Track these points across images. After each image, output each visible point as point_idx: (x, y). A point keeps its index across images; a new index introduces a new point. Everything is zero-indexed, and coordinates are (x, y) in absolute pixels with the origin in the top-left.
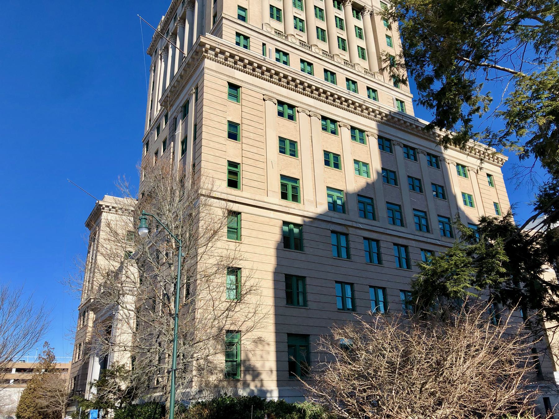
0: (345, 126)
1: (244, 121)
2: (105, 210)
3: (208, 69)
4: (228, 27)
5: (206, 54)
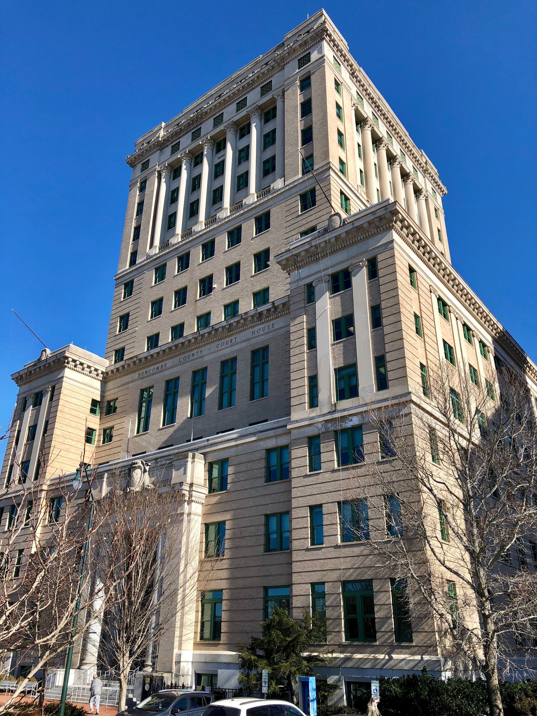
1: (424, 315)
2: (69, 365)
3: (396, 243)
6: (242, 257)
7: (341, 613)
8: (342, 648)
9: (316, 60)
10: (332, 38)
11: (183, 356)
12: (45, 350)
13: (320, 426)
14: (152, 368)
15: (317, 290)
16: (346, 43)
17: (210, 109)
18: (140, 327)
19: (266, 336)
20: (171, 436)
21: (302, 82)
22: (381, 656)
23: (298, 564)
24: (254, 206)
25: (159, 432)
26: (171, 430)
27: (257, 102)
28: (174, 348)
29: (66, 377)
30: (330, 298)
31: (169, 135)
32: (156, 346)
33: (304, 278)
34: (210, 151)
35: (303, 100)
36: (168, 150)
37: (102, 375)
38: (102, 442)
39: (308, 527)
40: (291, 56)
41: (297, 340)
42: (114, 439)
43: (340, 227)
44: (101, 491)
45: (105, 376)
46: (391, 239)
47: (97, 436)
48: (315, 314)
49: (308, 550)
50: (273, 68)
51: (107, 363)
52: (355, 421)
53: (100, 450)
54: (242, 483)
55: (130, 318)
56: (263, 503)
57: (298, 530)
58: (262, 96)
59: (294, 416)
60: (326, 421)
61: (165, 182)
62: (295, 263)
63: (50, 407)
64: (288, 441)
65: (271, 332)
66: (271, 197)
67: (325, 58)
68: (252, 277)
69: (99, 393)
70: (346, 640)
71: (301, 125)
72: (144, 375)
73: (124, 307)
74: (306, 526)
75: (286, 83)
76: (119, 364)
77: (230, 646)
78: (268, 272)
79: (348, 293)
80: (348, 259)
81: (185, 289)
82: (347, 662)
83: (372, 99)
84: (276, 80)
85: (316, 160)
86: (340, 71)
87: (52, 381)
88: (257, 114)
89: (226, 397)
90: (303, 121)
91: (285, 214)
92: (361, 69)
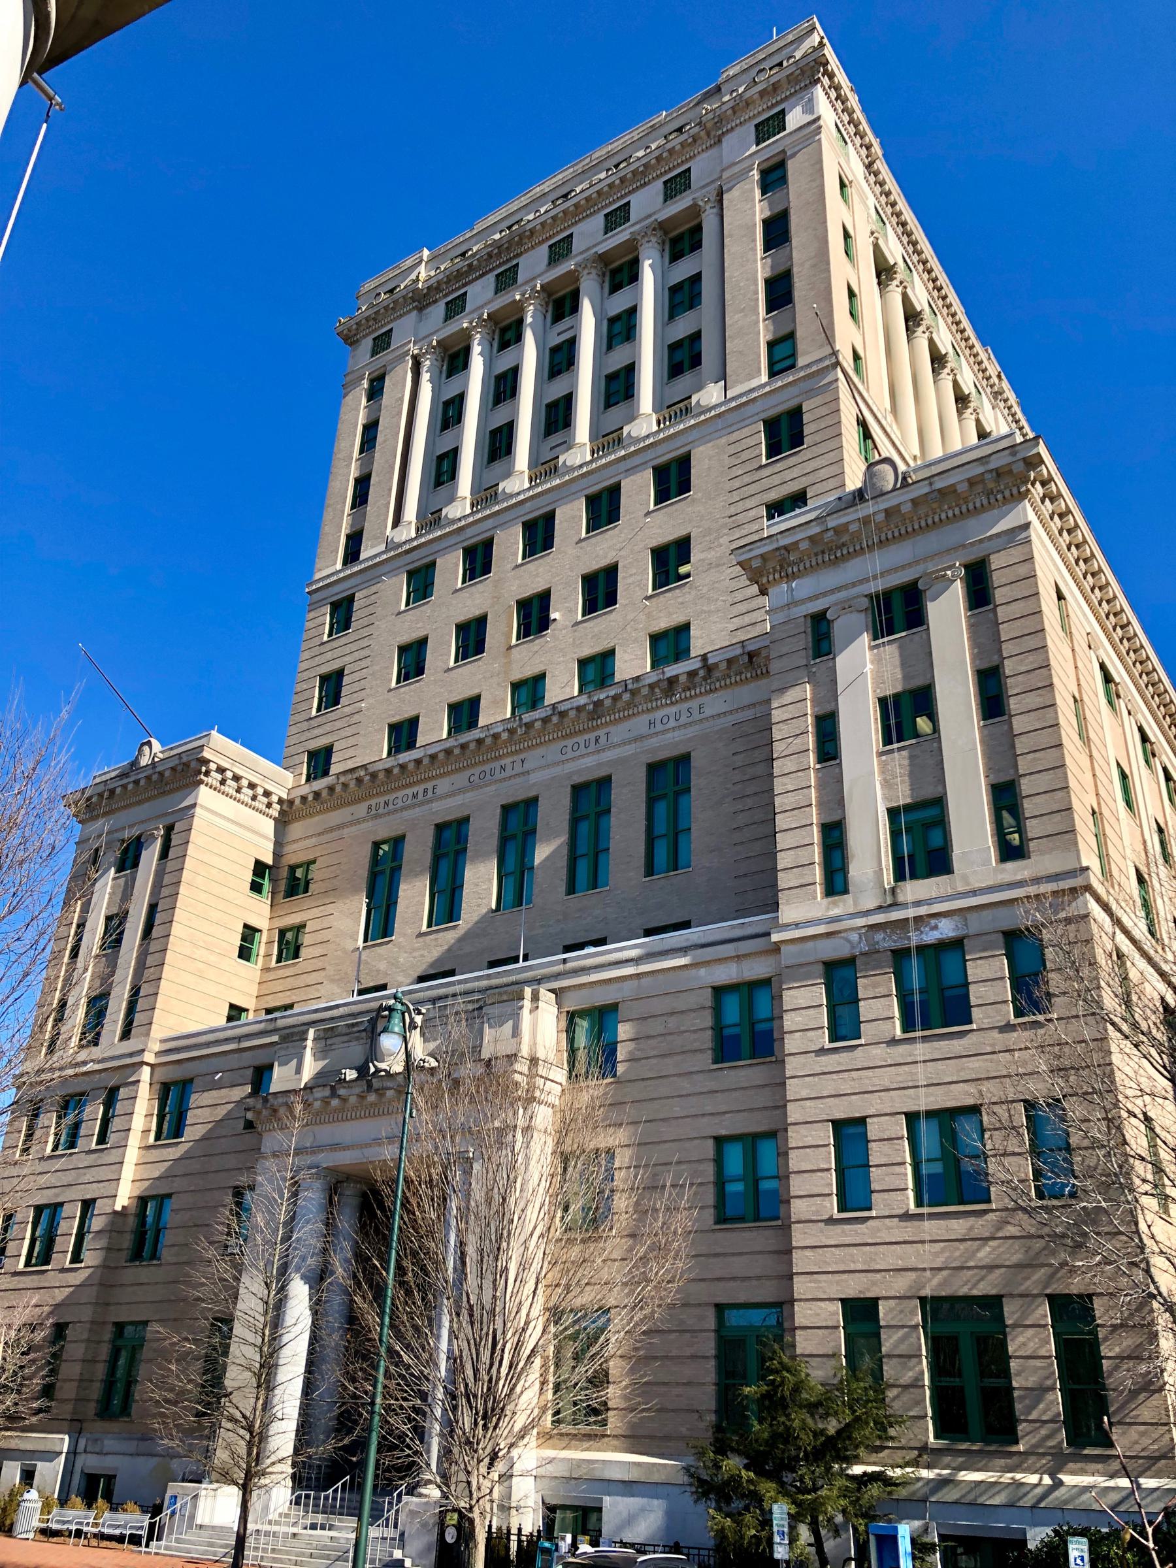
1: (1085, 698)
2: (209, 780)
6: (622, 553)
7: (922, 1373)
8: (924, 1455)
9: (801, 128)
11: (477, 770)
12: (149, 744)
13: (854, 937)
14: (400, 794)
15: (839, 629)
17: (543, 224)
18: (371, 701)
19: (683, 731)
20: (449, 950)
21: (764, 173)
22: (1033, 1479)
23: (808, 1253)
24: (651, 440)
25: (421, 939)
26: (448, 937)
27: (654, 213)
28: (457, 751)
29: (202, 807)
30: (872, 648)
31: (441, 276)
32: (411, 745)
33: (803, 601)
34: (540, 317)
35: (767, 214)
36: (439, 309)
37: (278, 807)
38: (274, 958)
39: (828, 1170)
40: (738, 114)
41: (789, 740)
42: (304, 952)
43: (894, 490)
44: (299, 1070)
45: (285, 807)
46: (1022, 522)
47: (263, 945)
48: (834, 681)
49: (831, 1221)
50: (695, 141)
51: (288, 778)
52: (946, 929)
53: (272, 975)
54: (654, 1061)
55: (346, 680)
56: (709, 1109)
57: (806, 1175)
58: (665, 201)
59: (788, 912)
60: (871, 927)
61: (431, 381)
62: (782, 567)
63: (160, 874)
64: (769, 969)
65: (695, 722)
66: (692, 422)
67: (821, 122)
68: (648, 598)
69: (271, 846)
70: (936, 1437)
71: (763, 268)
72: (381, 811)
73: (329, 656)
74: (825, 1166)
75: (725, 175)
76: (320, 784)
77: (636, 1441)
78: (686, 589)
79: (916, 638)
80: (917, 562)
81: (481, 621)
82: (945, 1490)
84: (701, 168)
85: (801, 346)
86: (847, 155)
87: (166, 814)
88: (654, 239)
89: (583, 867)
90: (769, 260)
91: (729, 462)
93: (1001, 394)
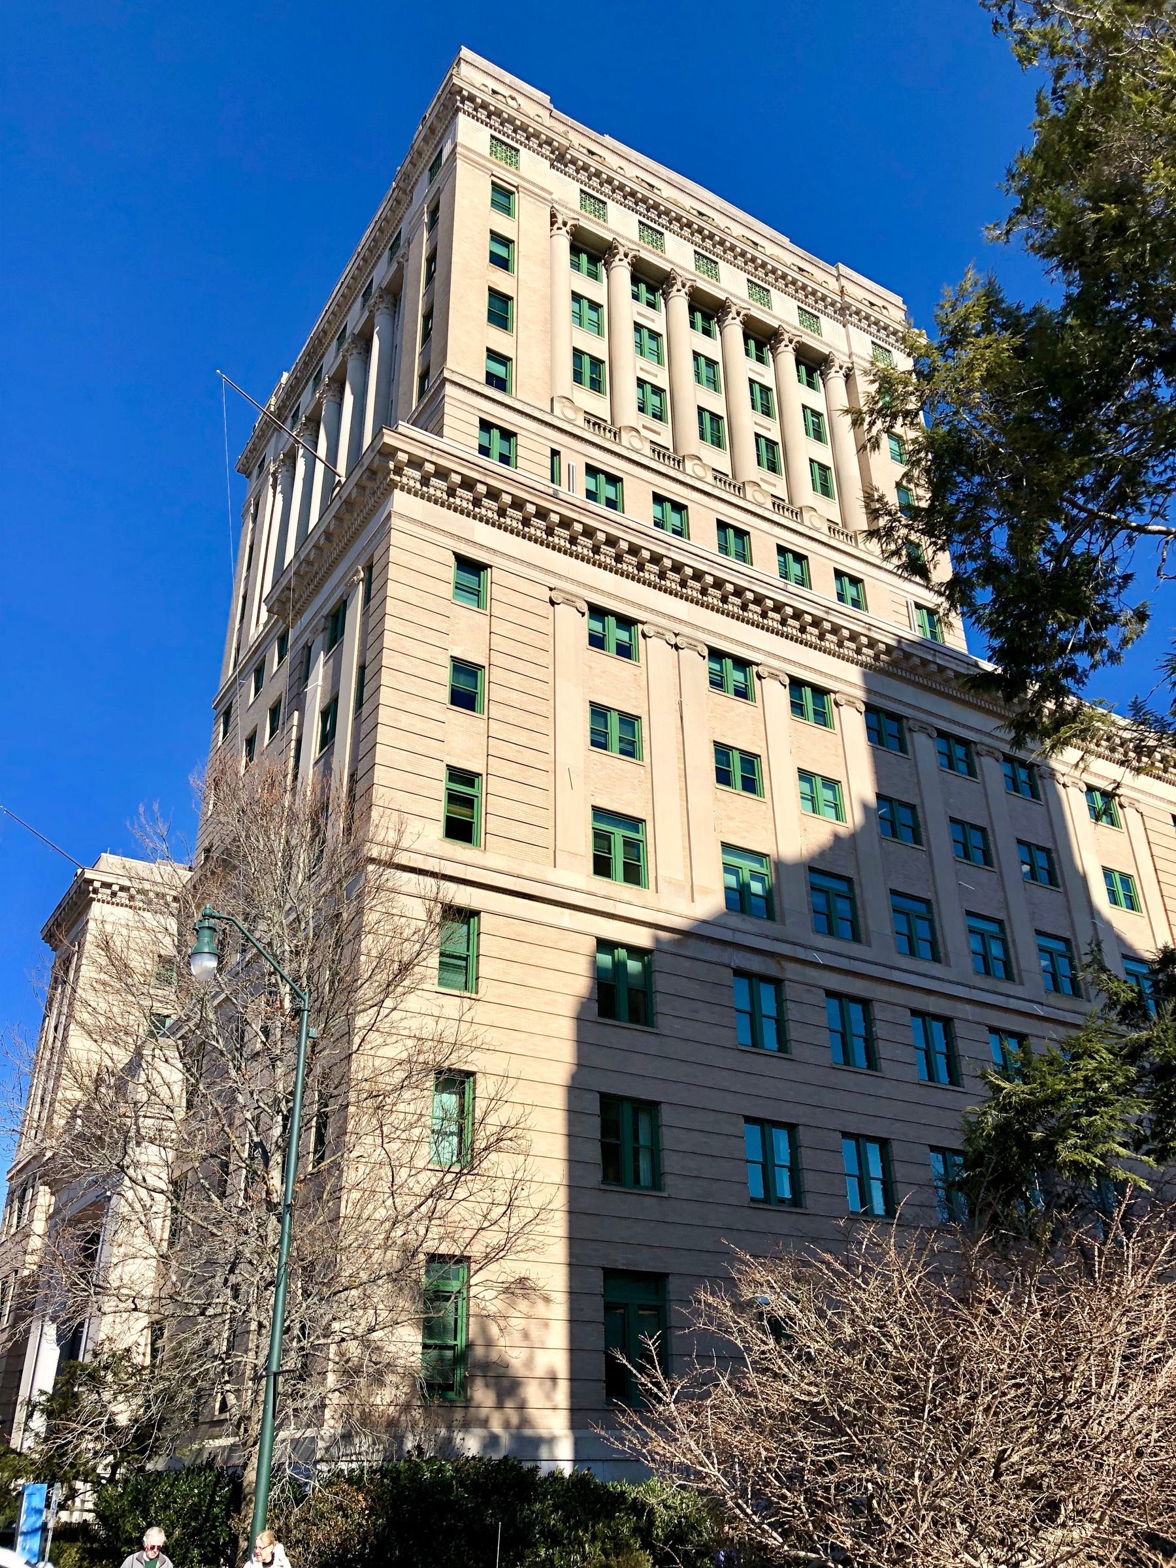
0: (774, 676)
1: (497, 659)
2: (100, 896)
3: (402, 516)
4: (459, 405)
5: (397, 478)
10: (479, 101)
16: (545, 98)
61: (281, 492)
83: (633, 194)
92: (607, 140)
93: (848, 308)
